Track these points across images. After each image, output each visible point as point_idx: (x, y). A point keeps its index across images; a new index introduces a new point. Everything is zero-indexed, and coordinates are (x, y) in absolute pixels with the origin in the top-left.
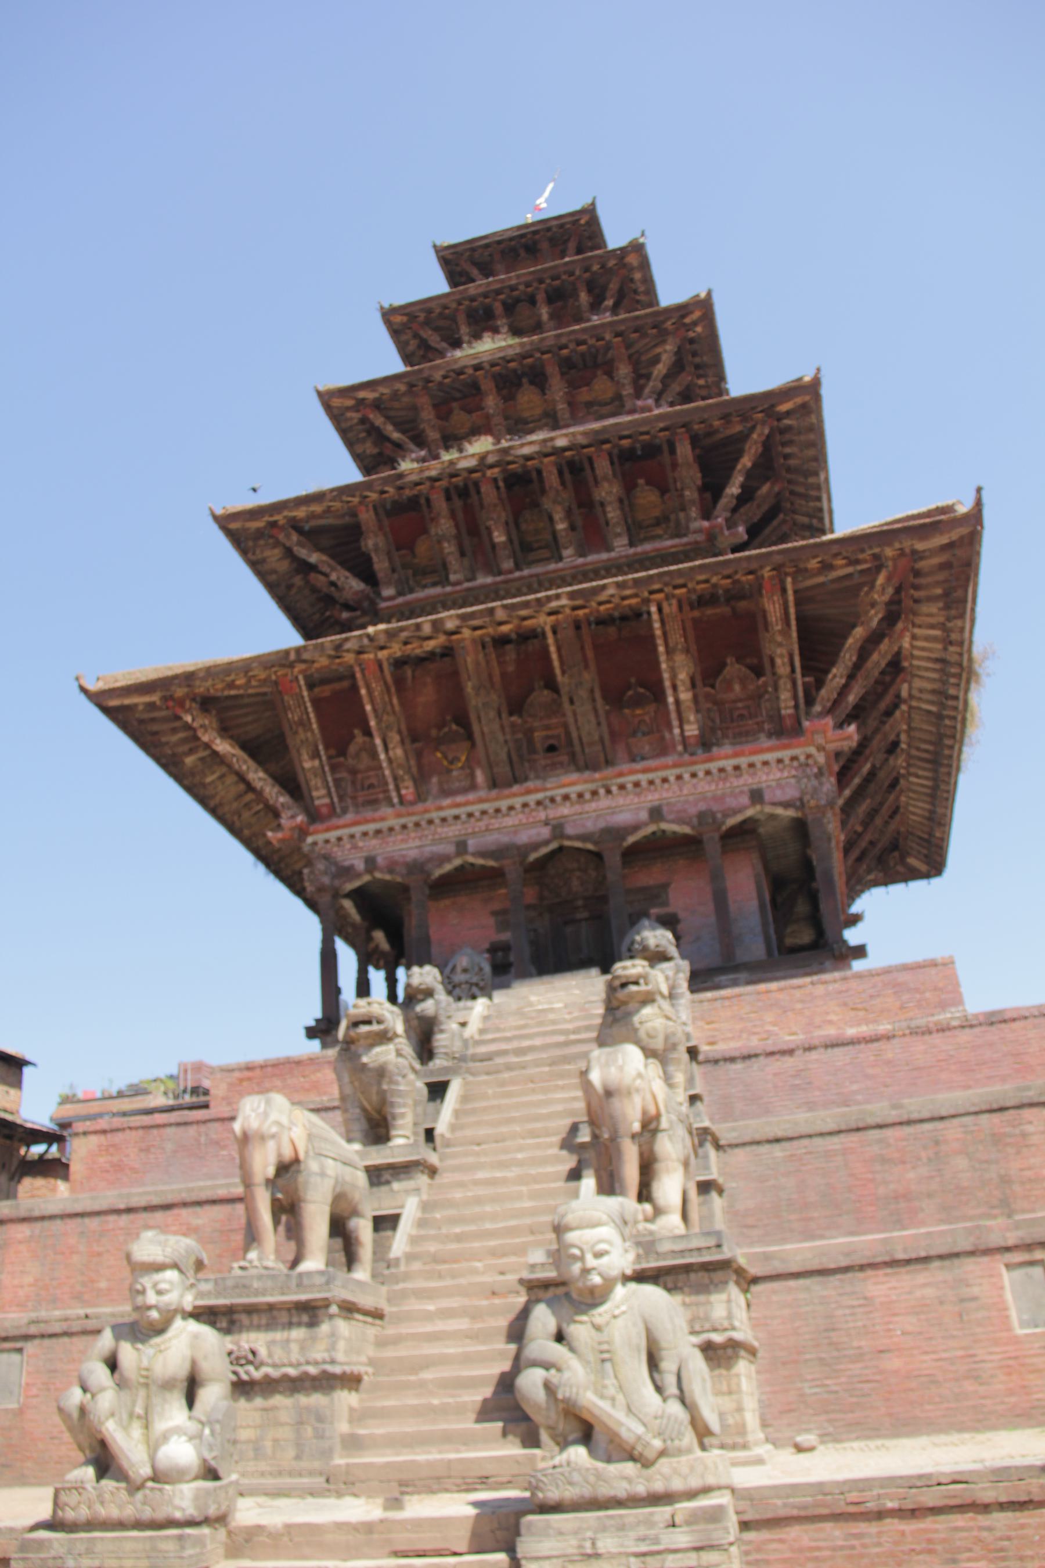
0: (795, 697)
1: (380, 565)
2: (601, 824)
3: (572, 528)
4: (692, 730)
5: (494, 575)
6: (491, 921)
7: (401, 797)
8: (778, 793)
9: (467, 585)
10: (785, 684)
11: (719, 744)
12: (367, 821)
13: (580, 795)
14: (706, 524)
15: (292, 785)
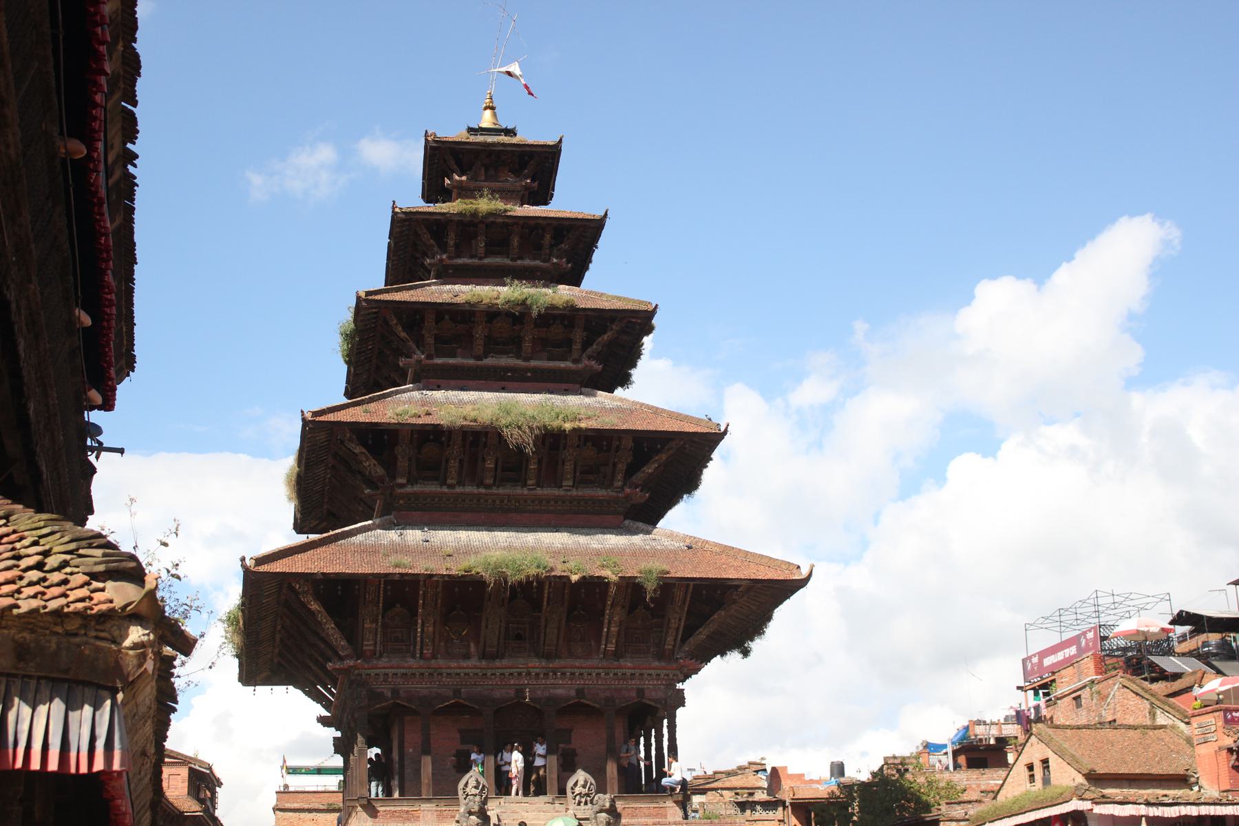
0: (675, 640)
1: (402, 464)
2: (546, 694)
3: (539, 469)
4: (611, 647)
5: (478, 487)
6: (458, 736)
7: (421, 653)
8: (653, 693)
9: (459, 490)
10: (672, 632)
11: (622, 657)
12: (398, 667)
13: (537, 674)
14: (628, 490)
15: (352, 636)
